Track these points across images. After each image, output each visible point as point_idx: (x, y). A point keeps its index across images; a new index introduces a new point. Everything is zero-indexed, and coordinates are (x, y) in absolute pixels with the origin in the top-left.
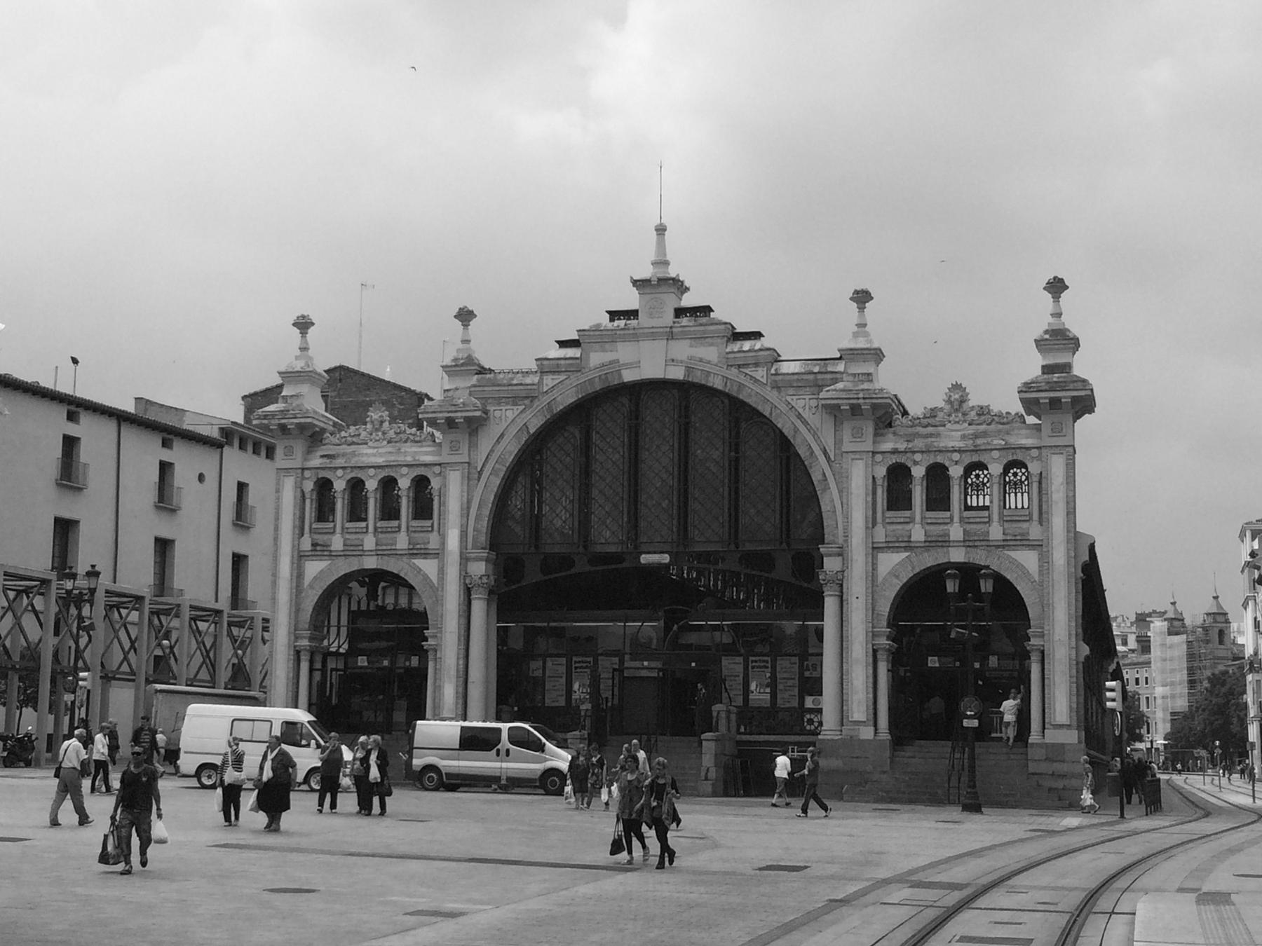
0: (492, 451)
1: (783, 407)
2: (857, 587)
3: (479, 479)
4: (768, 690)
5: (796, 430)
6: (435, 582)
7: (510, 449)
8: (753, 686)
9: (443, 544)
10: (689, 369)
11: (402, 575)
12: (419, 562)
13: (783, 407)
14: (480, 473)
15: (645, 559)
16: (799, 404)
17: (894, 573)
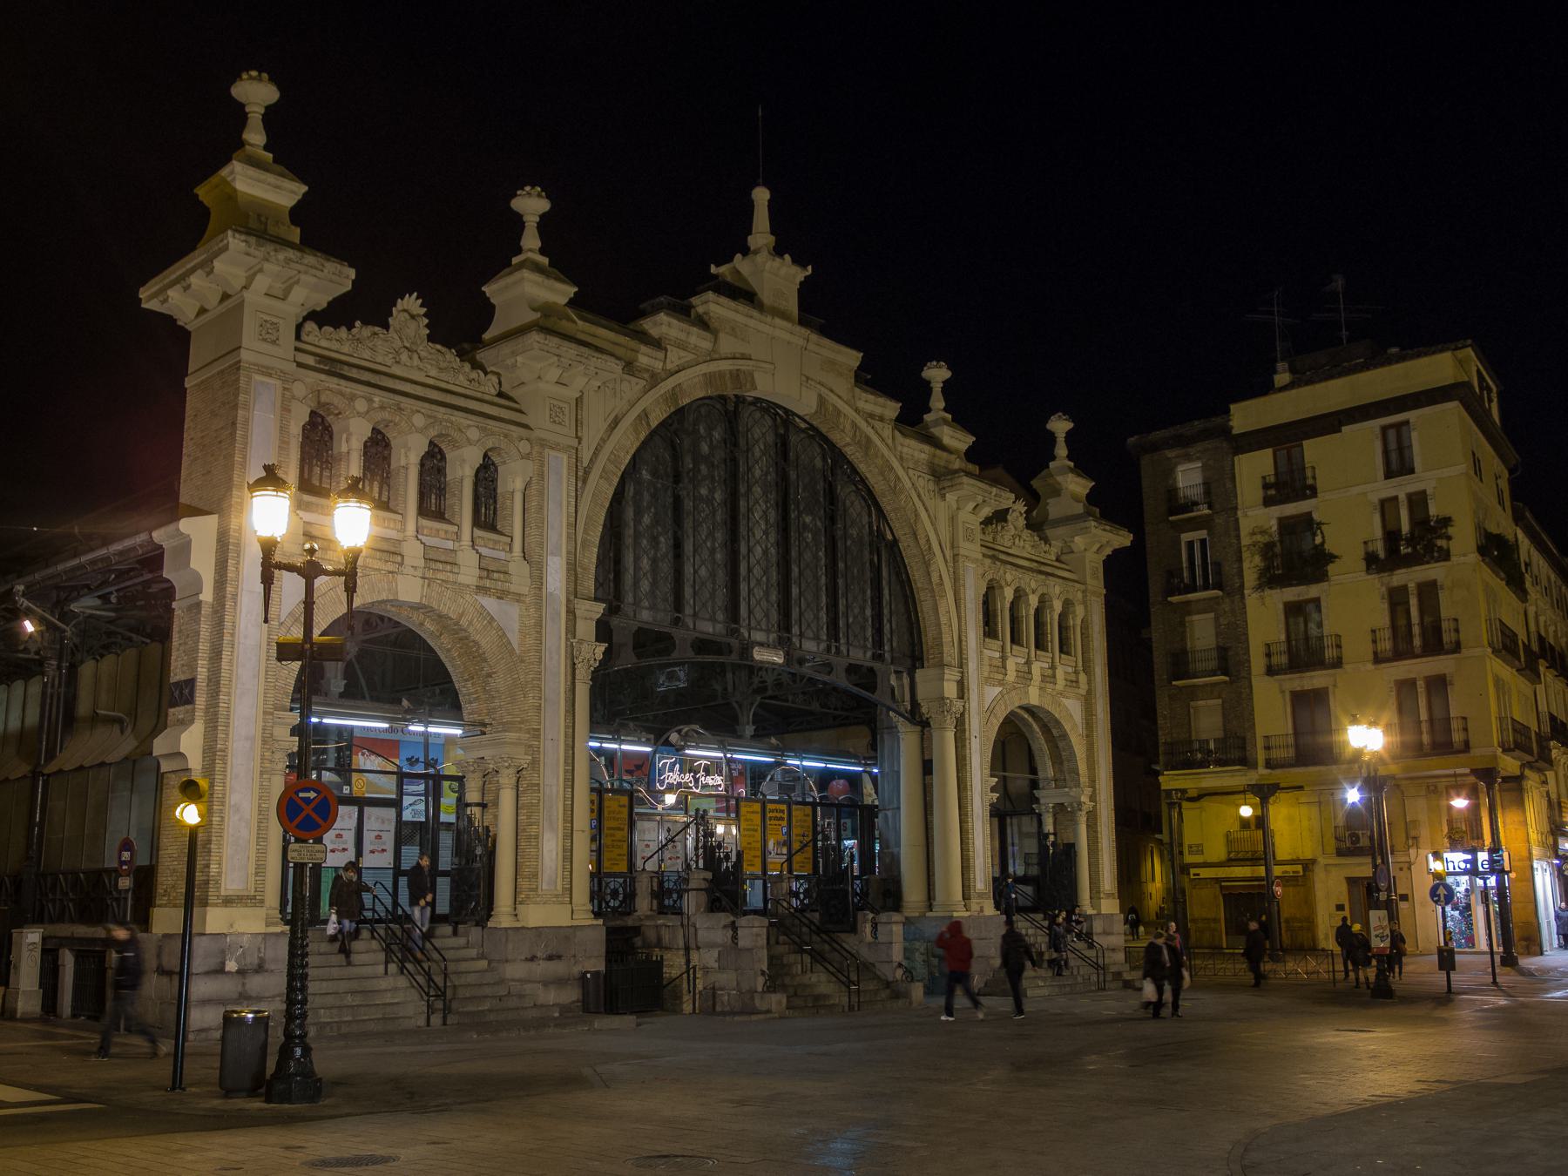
0: (604, 441)
1: (908, 485)
2: (974, 724)
3: (585, 481)
4: (785, 851)
5: (917, 515)
6: (516, 646)
7: (626, 442)
8: (771, 845)
9: (538, 580)
10: (822, 401)
11: (464, 622)
12: (490, 603)
13: (908, 485)
14: (587, 472)
15: (759, 655)
16: (921, 483)
17: (991, 711)
